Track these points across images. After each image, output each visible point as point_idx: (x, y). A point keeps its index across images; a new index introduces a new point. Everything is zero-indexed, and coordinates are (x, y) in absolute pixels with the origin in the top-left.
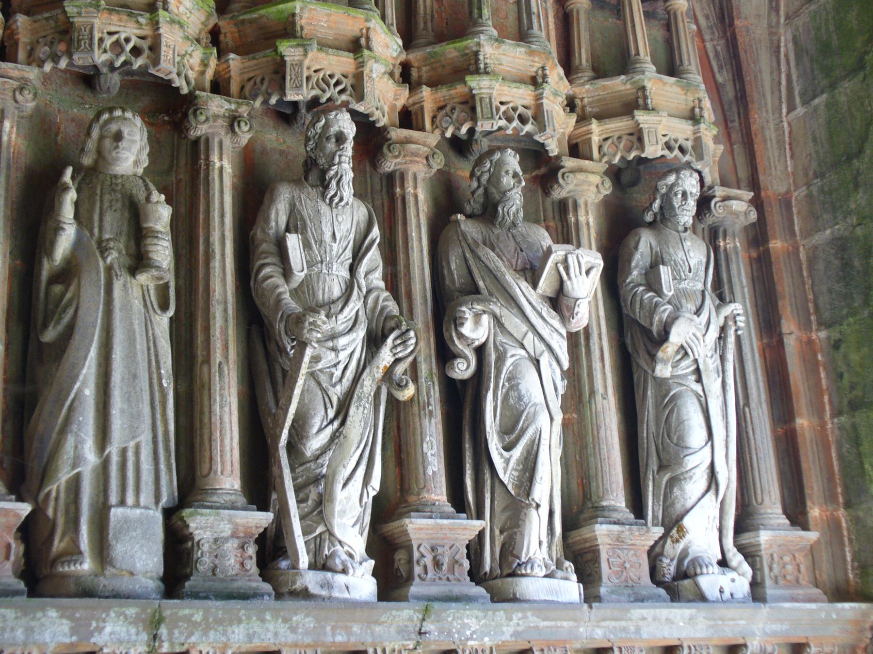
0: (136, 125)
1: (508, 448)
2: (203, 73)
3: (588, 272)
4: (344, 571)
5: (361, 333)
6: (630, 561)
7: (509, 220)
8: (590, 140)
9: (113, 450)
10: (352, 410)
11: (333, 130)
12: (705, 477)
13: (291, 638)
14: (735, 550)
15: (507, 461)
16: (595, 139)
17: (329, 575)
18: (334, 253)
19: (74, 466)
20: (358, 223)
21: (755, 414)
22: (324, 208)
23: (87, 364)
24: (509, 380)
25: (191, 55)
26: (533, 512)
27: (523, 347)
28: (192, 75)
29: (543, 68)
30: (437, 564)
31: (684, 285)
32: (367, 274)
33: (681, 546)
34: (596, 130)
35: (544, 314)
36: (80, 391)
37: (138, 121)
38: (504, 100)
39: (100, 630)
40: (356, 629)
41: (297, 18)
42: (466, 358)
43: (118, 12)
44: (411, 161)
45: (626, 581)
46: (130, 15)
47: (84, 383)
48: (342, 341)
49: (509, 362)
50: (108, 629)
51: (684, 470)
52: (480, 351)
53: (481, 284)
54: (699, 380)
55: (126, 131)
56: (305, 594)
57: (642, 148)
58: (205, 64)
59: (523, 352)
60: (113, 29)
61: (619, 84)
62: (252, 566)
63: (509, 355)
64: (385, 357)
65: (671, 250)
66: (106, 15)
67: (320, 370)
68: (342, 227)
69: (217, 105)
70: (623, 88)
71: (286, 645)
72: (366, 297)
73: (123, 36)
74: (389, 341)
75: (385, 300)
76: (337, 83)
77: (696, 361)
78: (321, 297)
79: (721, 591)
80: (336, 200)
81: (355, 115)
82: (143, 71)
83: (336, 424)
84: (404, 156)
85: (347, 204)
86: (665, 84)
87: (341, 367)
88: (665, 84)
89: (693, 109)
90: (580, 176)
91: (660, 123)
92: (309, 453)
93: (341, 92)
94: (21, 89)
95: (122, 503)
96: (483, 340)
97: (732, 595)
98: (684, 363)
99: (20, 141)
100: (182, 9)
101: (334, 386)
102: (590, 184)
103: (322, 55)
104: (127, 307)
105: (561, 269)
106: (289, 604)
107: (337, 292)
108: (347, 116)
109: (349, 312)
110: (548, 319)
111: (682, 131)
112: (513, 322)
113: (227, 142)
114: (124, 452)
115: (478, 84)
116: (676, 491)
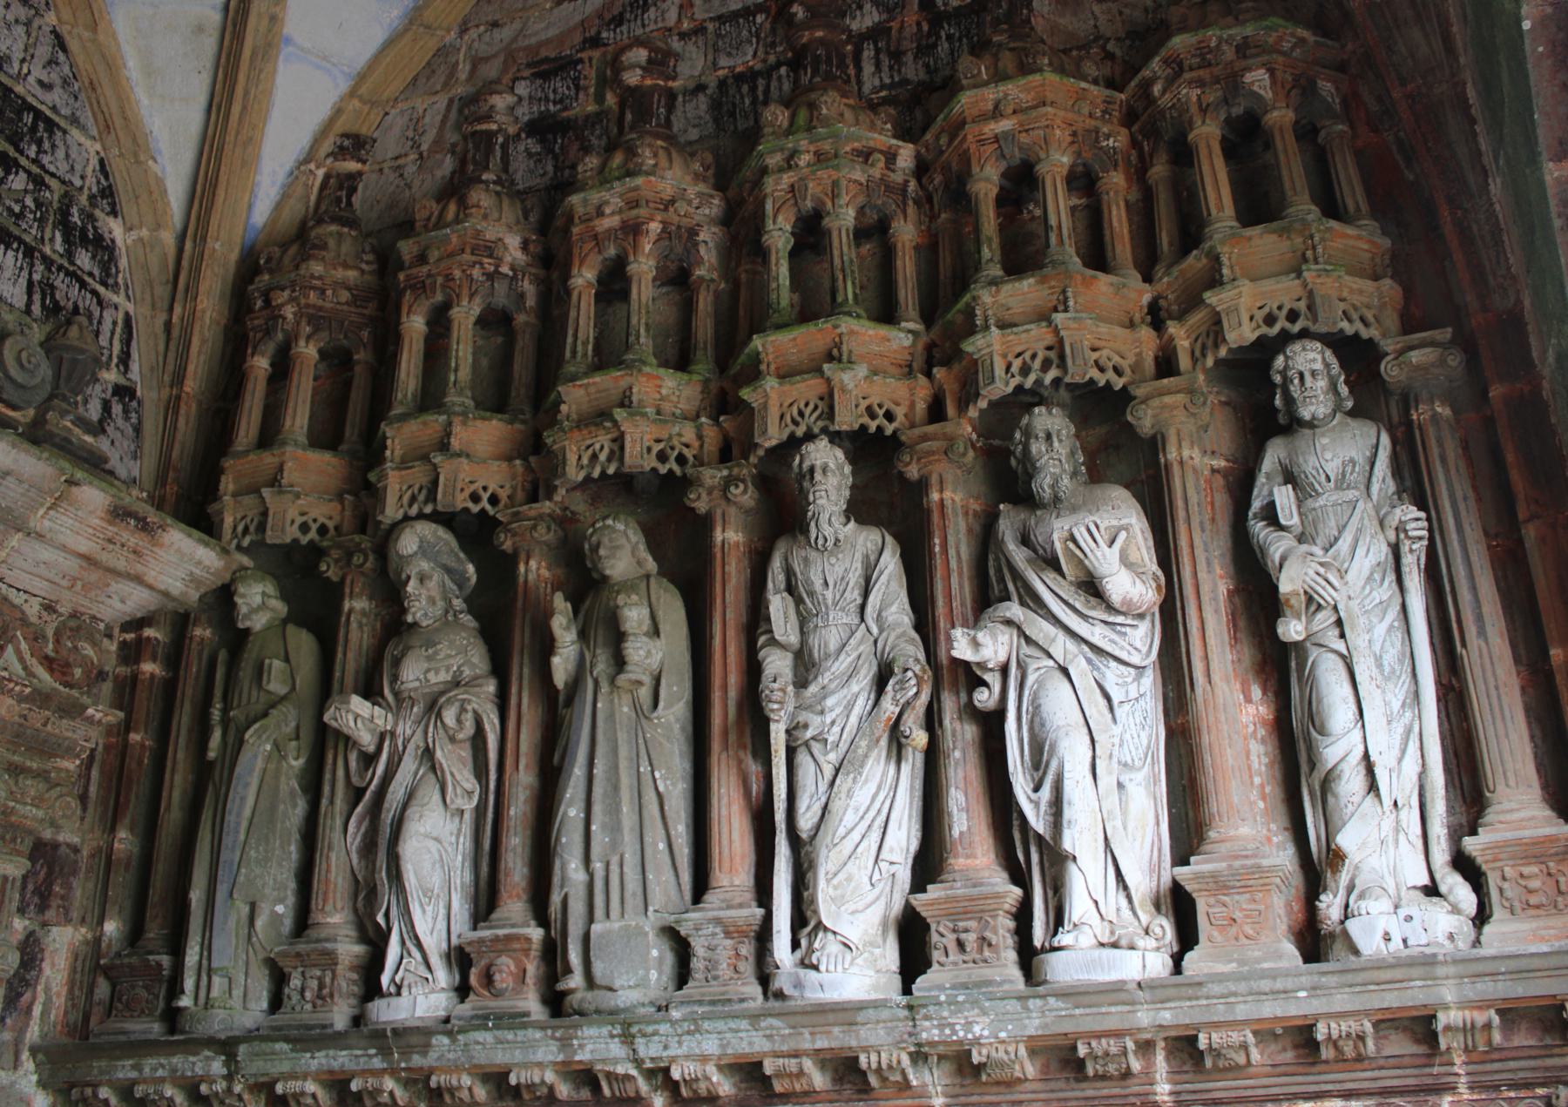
0: (614, 530)
1: (1036, 789)
2: (701, 446)
3: (1111, 543)
4: (816, 968)
5: (862, 683)
6: (1242, 910)
7: (1047, 494)
8: (1175, 348)
9: (598, 866)
10: (838, 781)
11: (806, 466)
12: (1363, 772)
13: (767, 1046)
14: (1448, 869)
15: (1037, 804)
16: (1183, 344)
17: (802, 972)
18: (830, 602)
19: (562, 887)
20: (867, 556)
21: (1475, 656)
22: (813, 555)
23: (572, 783)
24: (1033, 701)
25: (680, 435)
26: (1072, 868)
27: (1050, 656)
28: (688, 453)
29: (1064, 292)
30: (961, 945)
31: (1321, 501)
32: (879, 615)
33: (1344, 878)
34: (1181, 335)
35: (1078, 605)
36: (565, 813)
37: (620, 526)
38: (1019, 349)
39: (581, 1046)
40: (836, 1030)
41: (763, 356)
42: (985, 684)
43: (587, 426)
44: (930, 463)
45: (1237, 939)
46: (596, 425)
47: (569, 806)
48: (830, 702)
49: (1031, 678)
50: (589, 1047)
51: (1330, 766)
52: (1004, 670)
53: (1011, 587)
54: (1342, 636)
55: (605, 540)
56: (780, 995)
57: (1224, 340)
58: (700, 437)
59: (1051, 663)
60: (589, 442)
61: (1195, 262)
62: (748, 968)
63: (1030, 670)
64: (889, 708)
65: (1301, 460)
66: (576, 434)
67: (813, 738)
68: (836, 568)
69: (712, 476)
70: (1200, 265)
71: (765, 1054)
72: (876, 642)
73: (597, 446)
74: (889, 688)
75: (898, 637)
76: (816, 407)
77: (1335, 608)
78: (816, 655)
79: (1387, 938)
80: (820, 542)
81: (835, 438)
82: (617, 474)
83: (824, 800)
84: (919, 459)
85: (837, 540)
86: (1250, 239)
87: (836, 729)
88: (1250, 239)
89: (1304, 255)
90: (1155, 402)
91: (1240, 295)
92: (804, 836)
93: (818, 418)
94: (534, 527)
95: (608, 916)
96: (1002, 657)
97: (1405, 941)
98: (1320, 616)
99: (560, 572)
100: (664, 392)
101: (826, 753)
102: (1173, 408)
103: (787, 387)
104: (611, 717)
105: (1071, 545)
106: (774, 1004)
107: (833, 645)
108: (823, 443)
109: (842, 664)
110: (1085, 611)
111: (1283, 292)
112: (1040, 629)
113: (732, 511)
114: (608, 865)
115: (974, 346)
116: (1331, 800)
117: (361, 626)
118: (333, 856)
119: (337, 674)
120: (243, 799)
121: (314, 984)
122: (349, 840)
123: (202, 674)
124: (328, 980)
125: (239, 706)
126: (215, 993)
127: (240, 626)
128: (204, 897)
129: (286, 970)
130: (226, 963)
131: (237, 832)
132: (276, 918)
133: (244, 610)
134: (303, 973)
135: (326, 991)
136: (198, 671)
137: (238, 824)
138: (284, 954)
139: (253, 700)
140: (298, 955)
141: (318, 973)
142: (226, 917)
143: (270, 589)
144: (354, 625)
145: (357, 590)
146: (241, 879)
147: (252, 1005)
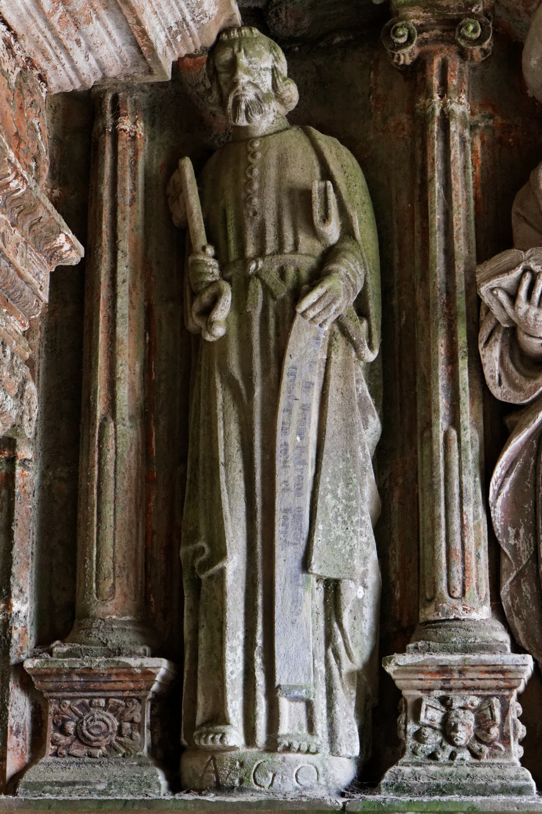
117: (463, 141)
118: (469, 509)
119: (437, 218)
120: (305, 408)
121: (470, 718)
122: (493, 487)
123: (140, 195)
124: (497, 713)
125: (261, 253)
126: (284, 729)
127: (242, 121)
128: (242, 567)
129: (410, 694)
130: (301, 680)
131: (304, 463)
132: (359, 602)
133: (250, 95)
134: (444, 701)
135: (495, 732)
136: (135, 188)
137: (302, 449)
138: (404, 669)
139: (288, 248)
140: (444, 669)
141: (477, 702)
142: (296, 601)
143: (283, 66)
144: (455, 139)
145: (453, 82)
146: (318, 539)
147: (344, 751)
